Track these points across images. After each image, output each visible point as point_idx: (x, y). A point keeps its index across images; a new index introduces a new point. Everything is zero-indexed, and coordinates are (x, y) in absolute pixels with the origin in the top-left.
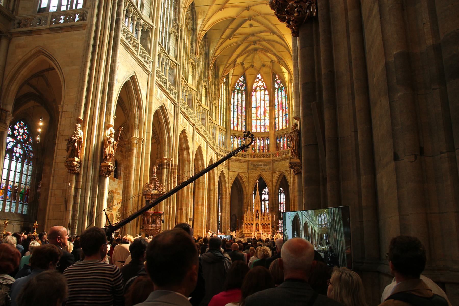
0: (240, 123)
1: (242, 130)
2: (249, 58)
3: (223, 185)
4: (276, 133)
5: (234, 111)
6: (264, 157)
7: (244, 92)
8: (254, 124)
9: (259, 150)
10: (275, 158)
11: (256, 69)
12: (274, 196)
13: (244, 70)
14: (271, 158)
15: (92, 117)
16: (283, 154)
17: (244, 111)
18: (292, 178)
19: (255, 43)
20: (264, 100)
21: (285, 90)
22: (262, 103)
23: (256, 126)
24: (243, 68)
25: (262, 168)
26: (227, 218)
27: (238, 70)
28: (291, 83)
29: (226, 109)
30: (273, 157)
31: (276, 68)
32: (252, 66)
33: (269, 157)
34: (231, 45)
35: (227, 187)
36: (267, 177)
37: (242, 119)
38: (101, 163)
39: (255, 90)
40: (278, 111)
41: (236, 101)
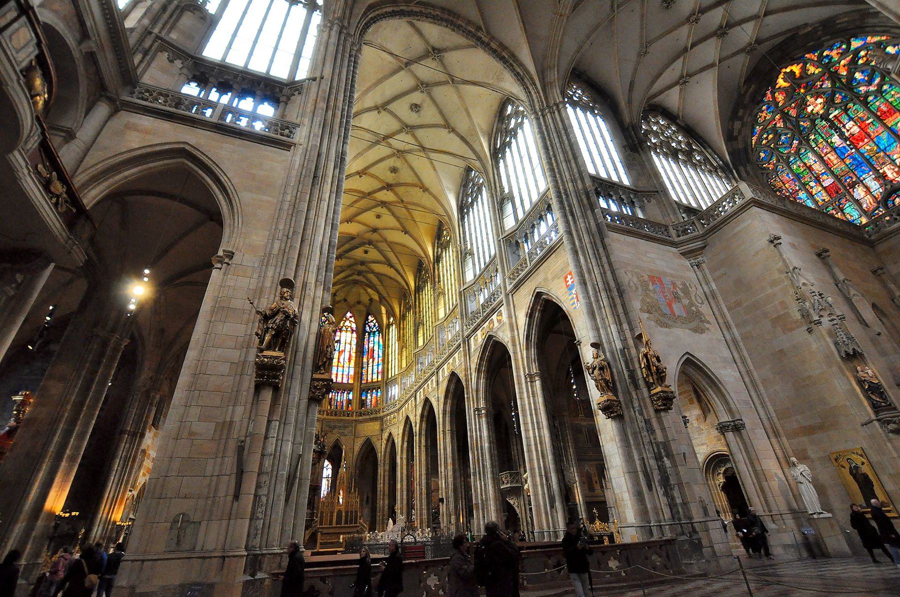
14: (354, 418)
18: (384, 445)
19: (359, 273)
22: (348, 346)
32: (345, 300)
39: (341, 331)
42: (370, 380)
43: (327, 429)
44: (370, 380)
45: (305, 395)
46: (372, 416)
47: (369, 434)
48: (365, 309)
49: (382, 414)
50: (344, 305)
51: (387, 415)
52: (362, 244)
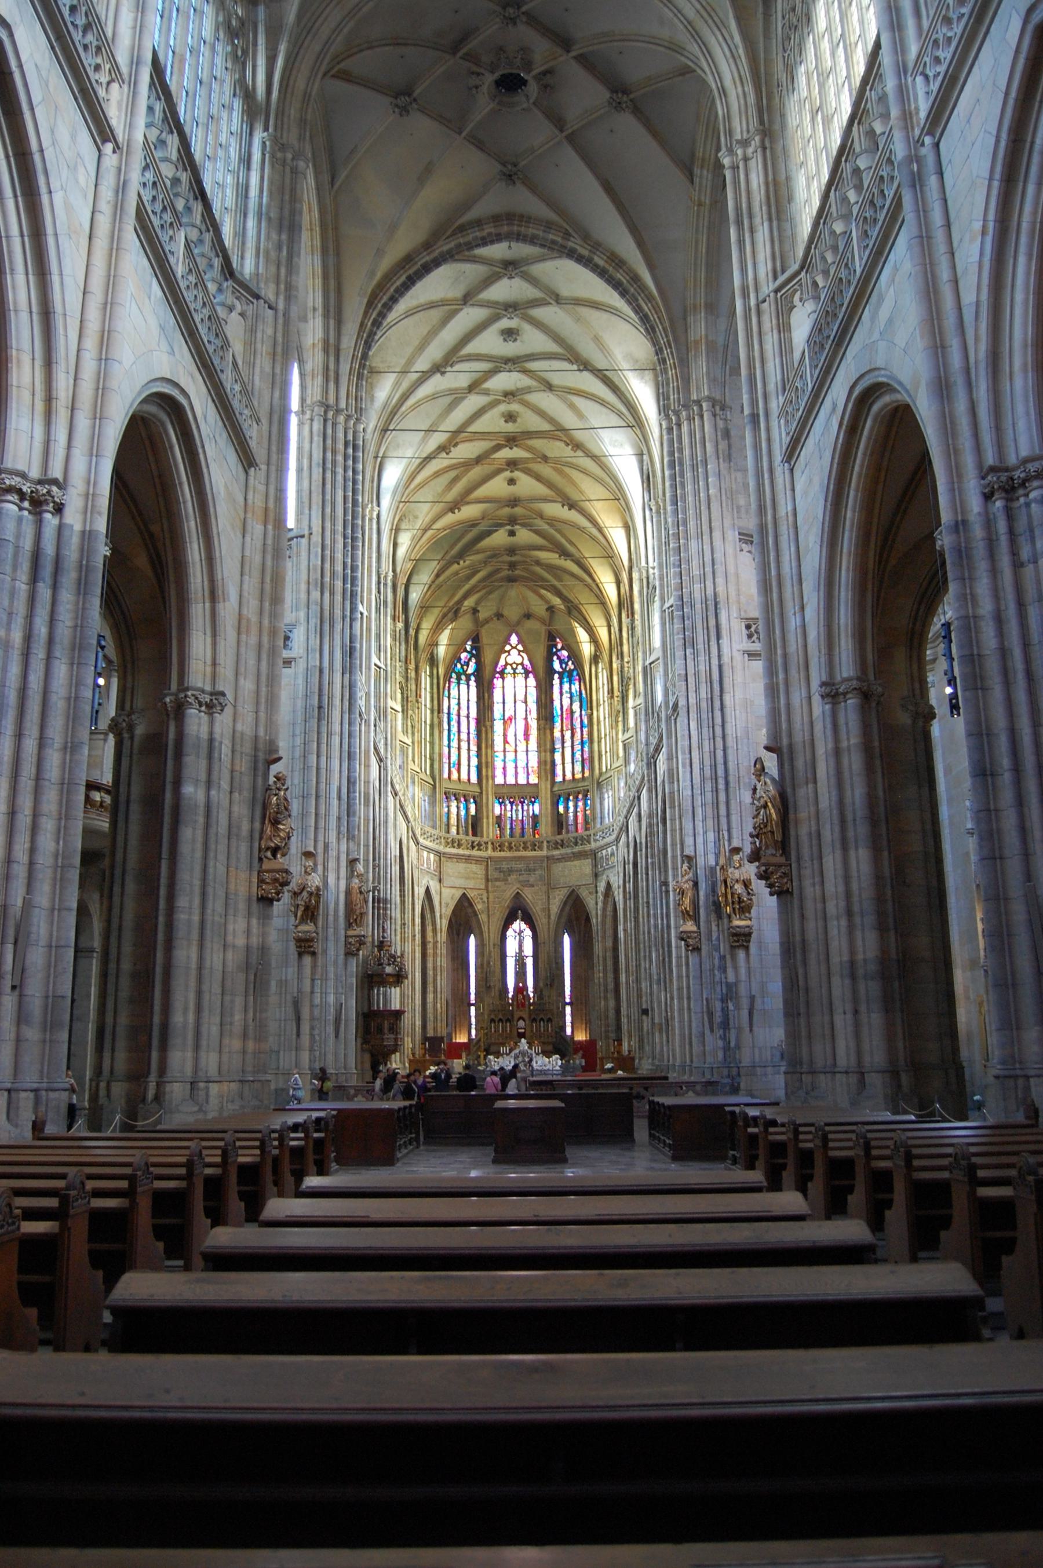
1: (469, 780)
2: (492, 596)
3: (429, 921)
4: (556, 789)
5: (449, 730)
6: (525, 848)
7: (473, 678)
8: (499, 764)
9: (511, 828)
10: (556, 853)
11: (508, 623)
12: (552, 949)
13: (478, 624)
14: (544, 853)
15: (326, 846)
16: (576, 844)
18: (600, 904)
19: (512, 566)
20: (526, 702)
21: (581, 679)
22: (521, 707)
23: (504, 768)
25: (521, 878)
26: (439, 1005)
27: (465, 623)
28: (596, 663)
29: (432, 726)
30: (548, 847)
31: (558, 626)
32: (499, 616)
33: (541, 848)
34: (457, 573)
35: (438, 927)
37: (469, 749)
38: (346, 930)
39: (502, 674)
40: (562, 731)
41: (454, 702)
42: (569, 776)
43: (496, 875)
44: (569, 776)
45: (342, 951)
46: (577, 849)
47: (574, 882)
48: (543, 630)
49: (593, 845)
50: (496, 624)
51: (602, 848)
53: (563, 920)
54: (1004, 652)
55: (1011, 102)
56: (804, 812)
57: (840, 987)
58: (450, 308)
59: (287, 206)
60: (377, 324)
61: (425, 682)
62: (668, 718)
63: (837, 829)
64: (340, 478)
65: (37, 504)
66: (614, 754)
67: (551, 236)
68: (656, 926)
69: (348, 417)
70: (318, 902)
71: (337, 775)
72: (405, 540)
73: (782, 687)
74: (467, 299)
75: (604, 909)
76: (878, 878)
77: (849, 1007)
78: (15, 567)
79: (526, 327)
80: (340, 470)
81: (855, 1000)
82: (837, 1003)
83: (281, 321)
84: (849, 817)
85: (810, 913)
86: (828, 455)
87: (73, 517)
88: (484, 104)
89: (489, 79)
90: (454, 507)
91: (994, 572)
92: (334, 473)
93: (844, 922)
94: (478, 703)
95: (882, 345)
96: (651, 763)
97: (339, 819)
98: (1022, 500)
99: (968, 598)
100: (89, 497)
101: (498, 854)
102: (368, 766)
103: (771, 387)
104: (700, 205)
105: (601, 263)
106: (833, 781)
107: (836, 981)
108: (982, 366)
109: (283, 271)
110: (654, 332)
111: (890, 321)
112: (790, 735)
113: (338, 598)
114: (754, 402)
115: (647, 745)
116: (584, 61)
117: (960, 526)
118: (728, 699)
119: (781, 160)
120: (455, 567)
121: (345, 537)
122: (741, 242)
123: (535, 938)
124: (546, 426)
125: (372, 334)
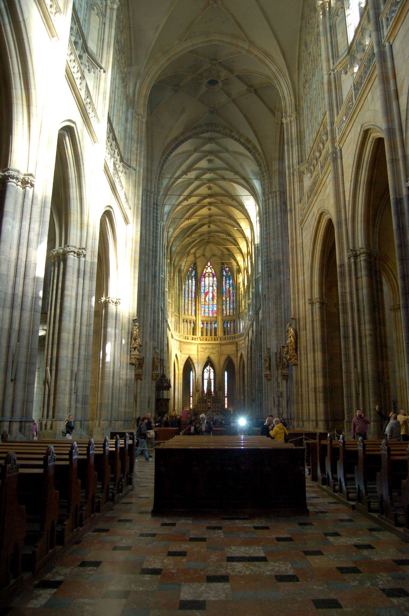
0: (190, 308)
14: (218, 342)
15: (146, 343)
17: (193, 296)
18: (238, 361)
20: (213, 286)
21: (233, 279)
22: (211, 288)
24: (195, 257)
27: (191, 258)
29: (179, 295)
30: (221, 340)
34: (189, 240)
36: (214, 358)
39: (205, 277)
40: (226, 297)
41: (187, 286)
42: (228, 314)
43: (201, 350)
44: (228, 314)
46: (231, 340)
49: (237, 340)
50: (202, 258)
52: (204, 225)
53: (225, 367)
54: (352, 303)
55: (358, 146)
56: (302, 340)
57: (312, 395)
58: (189, 154)
59: (139, 135)
60: (165, 161)
61: (177, 279)
62: (263, 299)
63: (312, 346)
64: (152, 216)
65: (79, 255)
66: (245, 306)
67: (226, 131)
68: (258, 371)
69: (155, 195)
70: (143, 363)
71: (149, 319)
72: (171, 230)
73: (297, 299)
74: (195, 150)
75: (240, 363)
76: (324, 362)
77: (314, 401)
78: (73, 273)
79: (216, 159)
80: (152, 213)
81: (316, 399)
82: (310, 400)
83: (137, 174)
84: (316, 342)
85: (303, 372)
86: (312, 228)
87: (88, 259)
88: (203, 89)
89: (206, 81)
90: (189, 218)
91: (350, 280)
92: (150, 214)
93: (313, 375)
94: (195, 286)
95: (326, 201)
96: (257, 313)
97: (150, 334)
98: (359, 260)
99: (344, 287)
100: (93, 252)
101: (201, 342)
102: (159, 314)
103: (296, 200)
104: (277, 124)
105: (243, 141)
106: (311, 330)
107: (310, 393)
108: (350, 220)
109: (138, 157)
110: (261, 166)
111: (329, 195)
112: (299, 315)
113: (151, 258)
114: (291, 205)
115: (256, 307)
116: (238, 77)
117: (342, 265)
118: (282, 295)
119: (302, 123)
120: (189, 238)
121: (153, 237)
122: (288, 150)
123: (214, 372)
124: (222, 192)
125: (163, 165)
